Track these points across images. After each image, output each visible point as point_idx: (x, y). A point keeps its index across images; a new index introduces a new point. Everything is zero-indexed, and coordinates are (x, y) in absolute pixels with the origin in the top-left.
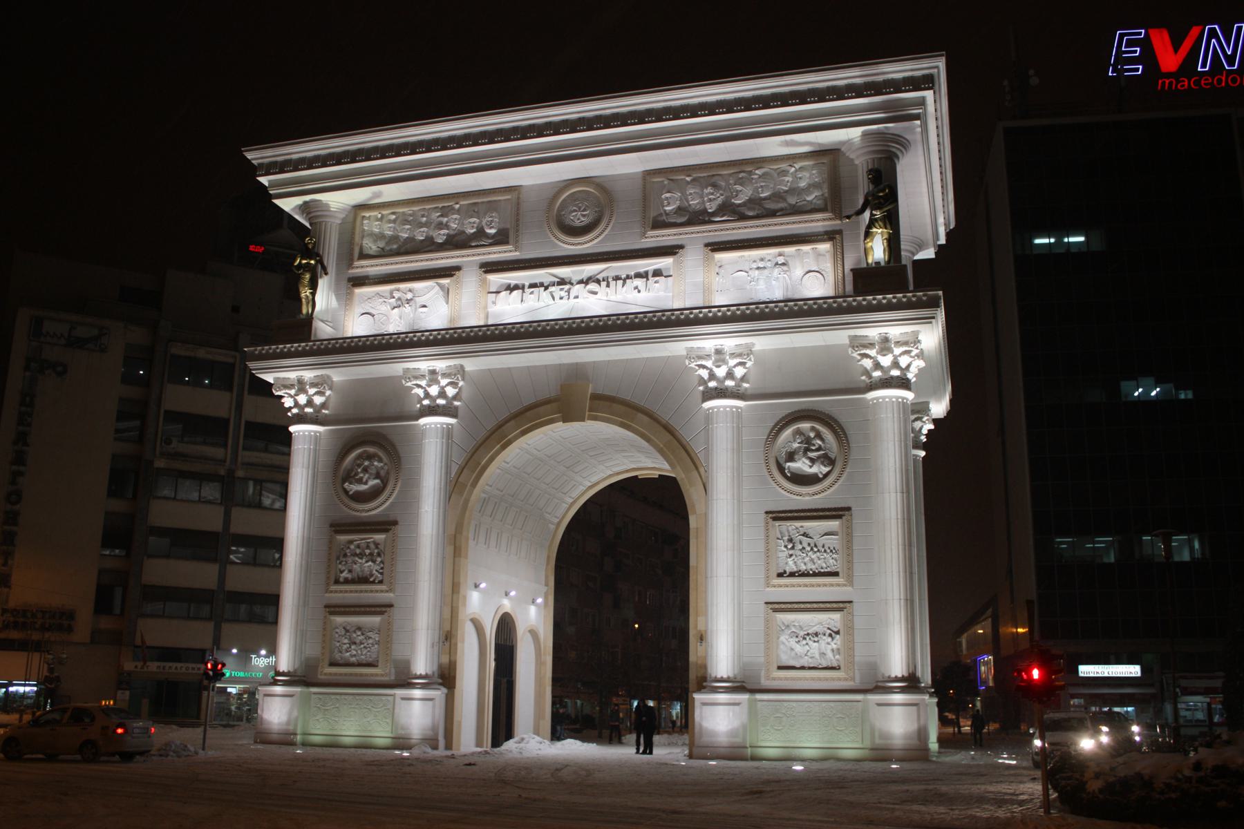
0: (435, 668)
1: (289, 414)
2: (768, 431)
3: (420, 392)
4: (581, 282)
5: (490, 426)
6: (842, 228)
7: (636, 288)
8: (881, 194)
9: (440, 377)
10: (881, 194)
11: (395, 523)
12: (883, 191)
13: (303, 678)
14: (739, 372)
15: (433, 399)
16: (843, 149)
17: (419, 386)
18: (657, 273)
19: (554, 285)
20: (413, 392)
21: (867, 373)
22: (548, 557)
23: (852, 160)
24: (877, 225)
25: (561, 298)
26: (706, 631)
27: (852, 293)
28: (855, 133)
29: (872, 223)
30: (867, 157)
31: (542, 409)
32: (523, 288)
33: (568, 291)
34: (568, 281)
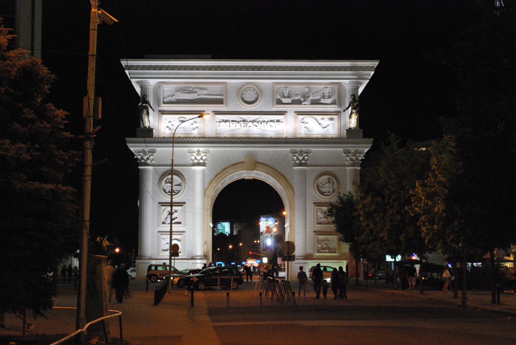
0: (203, 253)
1: (138, 161)
2: (314, 178)
3: (193, 158)
4: (251, 121)
5: (219, 170)
6: (341, 110)
7: (271, 125)
8: (355, 104)
9: (201, 153)
10: (355, 104)
11: (185, 203)
12: (356, 103)
13: (151, 257)
14: (306, 157)
15: (199, 160)
16: (342, 83)
17: (193, 155)
18: (278, 121)
19: (241, 121)
20: (190, 157)
21: (347, 161)
22: (211, 209)
23: (345, 87)
24: (353, 114)
25: (244, 127)
26: (295, 240)
27: (346, 138)
28: (347, 81)
29: (352, 113)
30: (350, 88)
31: (237, 165)
32: (229, 121)
33: (246, 124)
34: (246, 120)
